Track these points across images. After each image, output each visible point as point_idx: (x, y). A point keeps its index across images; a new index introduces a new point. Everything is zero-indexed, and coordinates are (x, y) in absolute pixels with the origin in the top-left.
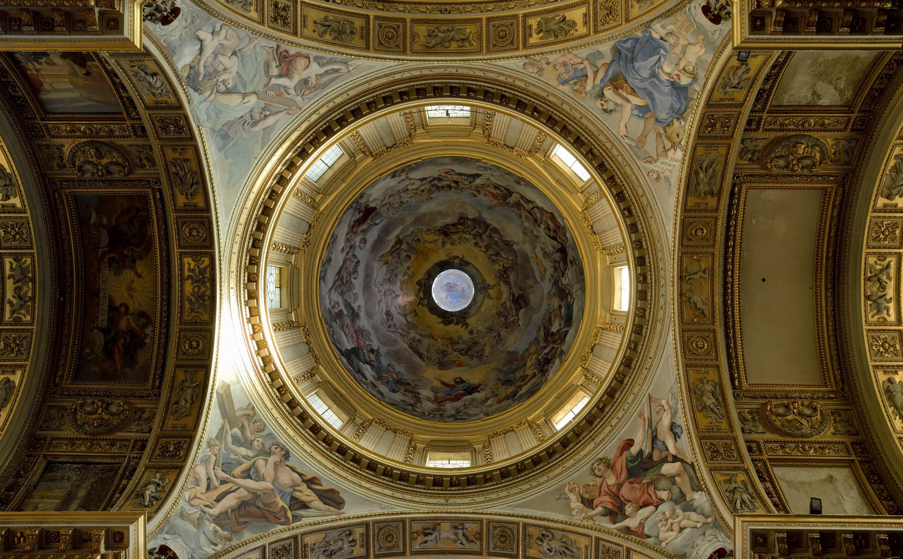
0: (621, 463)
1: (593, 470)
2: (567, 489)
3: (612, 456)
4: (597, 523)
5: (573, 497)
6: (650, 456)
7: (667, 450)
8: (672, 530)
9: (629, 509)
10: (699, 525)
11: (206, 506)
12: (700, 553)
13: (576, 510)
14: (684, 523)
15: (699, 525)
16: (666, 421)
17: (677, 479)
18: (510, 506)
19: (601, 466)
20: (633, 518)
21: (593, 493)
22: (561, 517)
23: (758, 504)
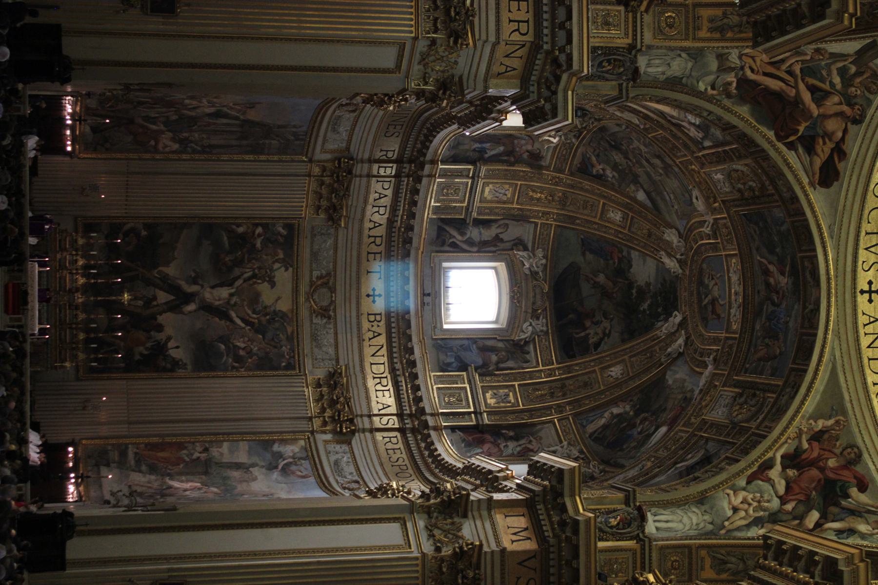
0: (846, 475)
1: (853, 446)
2: (841, 418)
3: (858, 468)
4: (789, 441)
5: (830, 422)
6: (837, 504)
7: (833, 521)
8: (742, 503)
9: (791, 473)
10: (726, 523)
11: (752, 70)
12: (690, 514)
13: (813, 423)
14: (743, 514)
15: (726, 523)
16: (863, 528)
17: (797, 522)
18: (835, 358)
19: (853, 455)
20: (780, 474)
21: (826, 443)
22: (810, 406)
23: (724, 576)
